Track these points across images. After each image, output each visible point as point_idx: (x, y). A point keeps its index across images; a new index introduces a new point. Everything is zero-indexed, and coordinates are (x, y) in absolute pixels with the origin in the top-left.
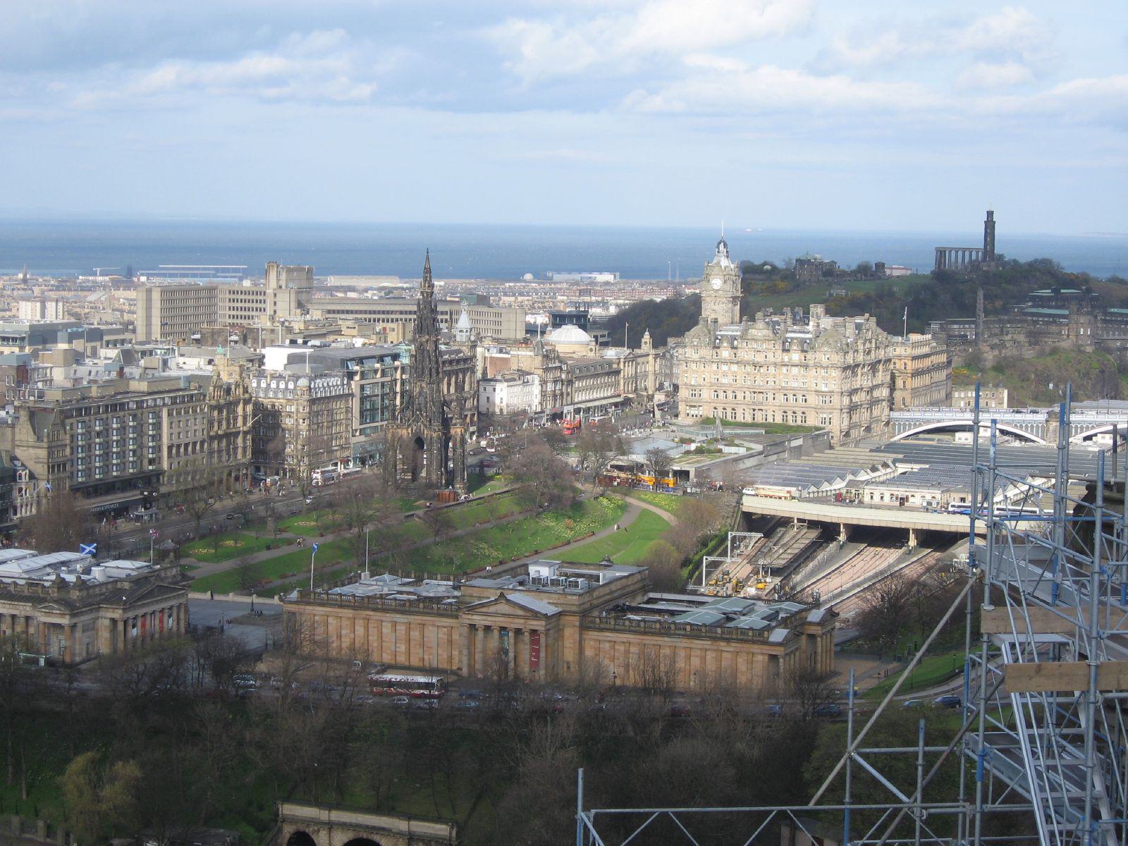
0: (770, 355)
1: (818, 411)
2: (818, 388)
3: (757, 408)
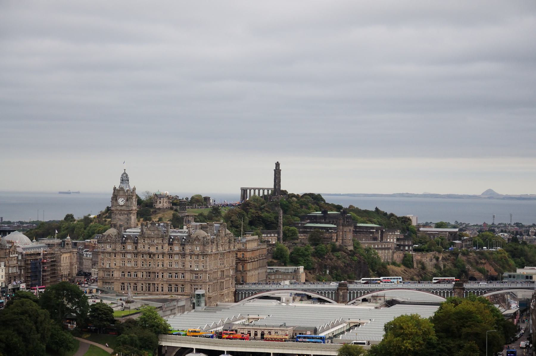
0: (160, 247)
1: (193, 284)
2: (192, 268)
3: (151, 282)
